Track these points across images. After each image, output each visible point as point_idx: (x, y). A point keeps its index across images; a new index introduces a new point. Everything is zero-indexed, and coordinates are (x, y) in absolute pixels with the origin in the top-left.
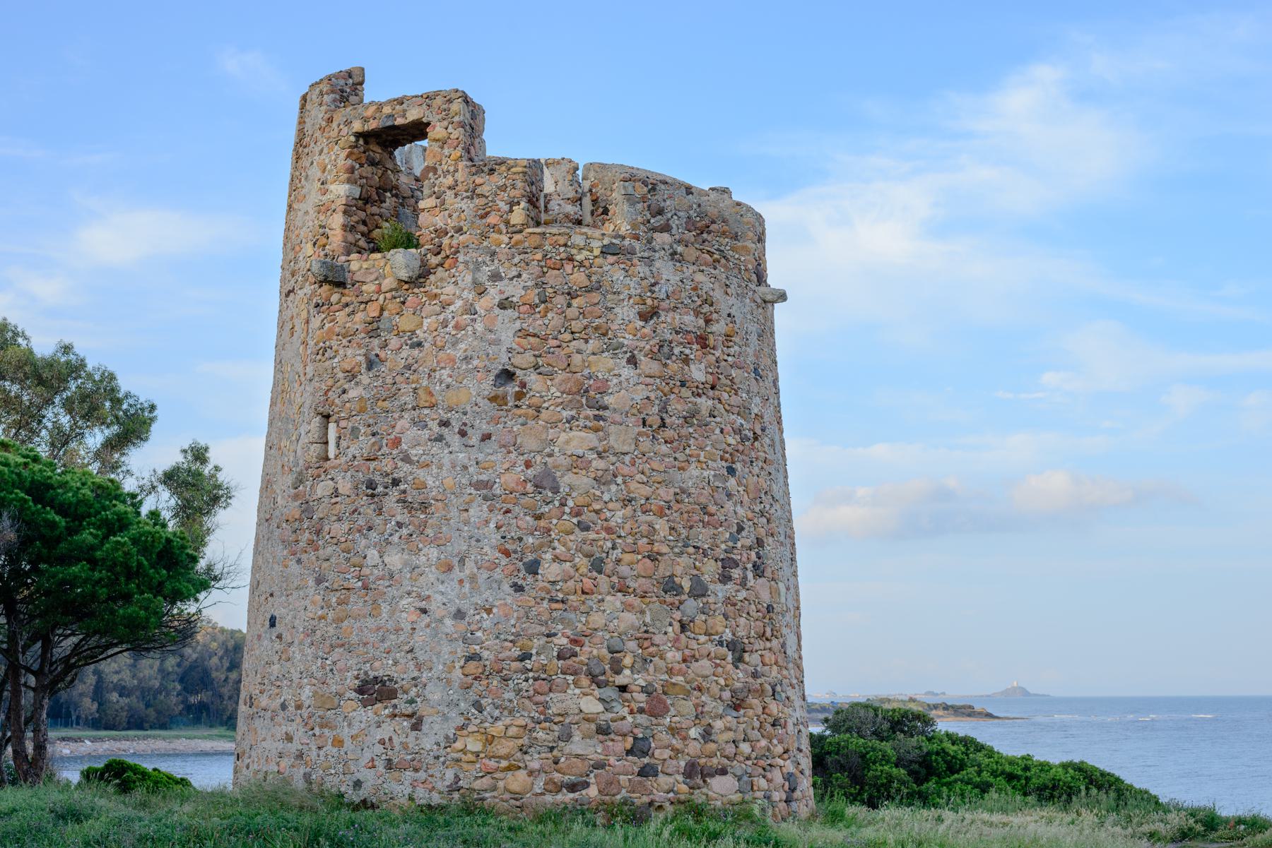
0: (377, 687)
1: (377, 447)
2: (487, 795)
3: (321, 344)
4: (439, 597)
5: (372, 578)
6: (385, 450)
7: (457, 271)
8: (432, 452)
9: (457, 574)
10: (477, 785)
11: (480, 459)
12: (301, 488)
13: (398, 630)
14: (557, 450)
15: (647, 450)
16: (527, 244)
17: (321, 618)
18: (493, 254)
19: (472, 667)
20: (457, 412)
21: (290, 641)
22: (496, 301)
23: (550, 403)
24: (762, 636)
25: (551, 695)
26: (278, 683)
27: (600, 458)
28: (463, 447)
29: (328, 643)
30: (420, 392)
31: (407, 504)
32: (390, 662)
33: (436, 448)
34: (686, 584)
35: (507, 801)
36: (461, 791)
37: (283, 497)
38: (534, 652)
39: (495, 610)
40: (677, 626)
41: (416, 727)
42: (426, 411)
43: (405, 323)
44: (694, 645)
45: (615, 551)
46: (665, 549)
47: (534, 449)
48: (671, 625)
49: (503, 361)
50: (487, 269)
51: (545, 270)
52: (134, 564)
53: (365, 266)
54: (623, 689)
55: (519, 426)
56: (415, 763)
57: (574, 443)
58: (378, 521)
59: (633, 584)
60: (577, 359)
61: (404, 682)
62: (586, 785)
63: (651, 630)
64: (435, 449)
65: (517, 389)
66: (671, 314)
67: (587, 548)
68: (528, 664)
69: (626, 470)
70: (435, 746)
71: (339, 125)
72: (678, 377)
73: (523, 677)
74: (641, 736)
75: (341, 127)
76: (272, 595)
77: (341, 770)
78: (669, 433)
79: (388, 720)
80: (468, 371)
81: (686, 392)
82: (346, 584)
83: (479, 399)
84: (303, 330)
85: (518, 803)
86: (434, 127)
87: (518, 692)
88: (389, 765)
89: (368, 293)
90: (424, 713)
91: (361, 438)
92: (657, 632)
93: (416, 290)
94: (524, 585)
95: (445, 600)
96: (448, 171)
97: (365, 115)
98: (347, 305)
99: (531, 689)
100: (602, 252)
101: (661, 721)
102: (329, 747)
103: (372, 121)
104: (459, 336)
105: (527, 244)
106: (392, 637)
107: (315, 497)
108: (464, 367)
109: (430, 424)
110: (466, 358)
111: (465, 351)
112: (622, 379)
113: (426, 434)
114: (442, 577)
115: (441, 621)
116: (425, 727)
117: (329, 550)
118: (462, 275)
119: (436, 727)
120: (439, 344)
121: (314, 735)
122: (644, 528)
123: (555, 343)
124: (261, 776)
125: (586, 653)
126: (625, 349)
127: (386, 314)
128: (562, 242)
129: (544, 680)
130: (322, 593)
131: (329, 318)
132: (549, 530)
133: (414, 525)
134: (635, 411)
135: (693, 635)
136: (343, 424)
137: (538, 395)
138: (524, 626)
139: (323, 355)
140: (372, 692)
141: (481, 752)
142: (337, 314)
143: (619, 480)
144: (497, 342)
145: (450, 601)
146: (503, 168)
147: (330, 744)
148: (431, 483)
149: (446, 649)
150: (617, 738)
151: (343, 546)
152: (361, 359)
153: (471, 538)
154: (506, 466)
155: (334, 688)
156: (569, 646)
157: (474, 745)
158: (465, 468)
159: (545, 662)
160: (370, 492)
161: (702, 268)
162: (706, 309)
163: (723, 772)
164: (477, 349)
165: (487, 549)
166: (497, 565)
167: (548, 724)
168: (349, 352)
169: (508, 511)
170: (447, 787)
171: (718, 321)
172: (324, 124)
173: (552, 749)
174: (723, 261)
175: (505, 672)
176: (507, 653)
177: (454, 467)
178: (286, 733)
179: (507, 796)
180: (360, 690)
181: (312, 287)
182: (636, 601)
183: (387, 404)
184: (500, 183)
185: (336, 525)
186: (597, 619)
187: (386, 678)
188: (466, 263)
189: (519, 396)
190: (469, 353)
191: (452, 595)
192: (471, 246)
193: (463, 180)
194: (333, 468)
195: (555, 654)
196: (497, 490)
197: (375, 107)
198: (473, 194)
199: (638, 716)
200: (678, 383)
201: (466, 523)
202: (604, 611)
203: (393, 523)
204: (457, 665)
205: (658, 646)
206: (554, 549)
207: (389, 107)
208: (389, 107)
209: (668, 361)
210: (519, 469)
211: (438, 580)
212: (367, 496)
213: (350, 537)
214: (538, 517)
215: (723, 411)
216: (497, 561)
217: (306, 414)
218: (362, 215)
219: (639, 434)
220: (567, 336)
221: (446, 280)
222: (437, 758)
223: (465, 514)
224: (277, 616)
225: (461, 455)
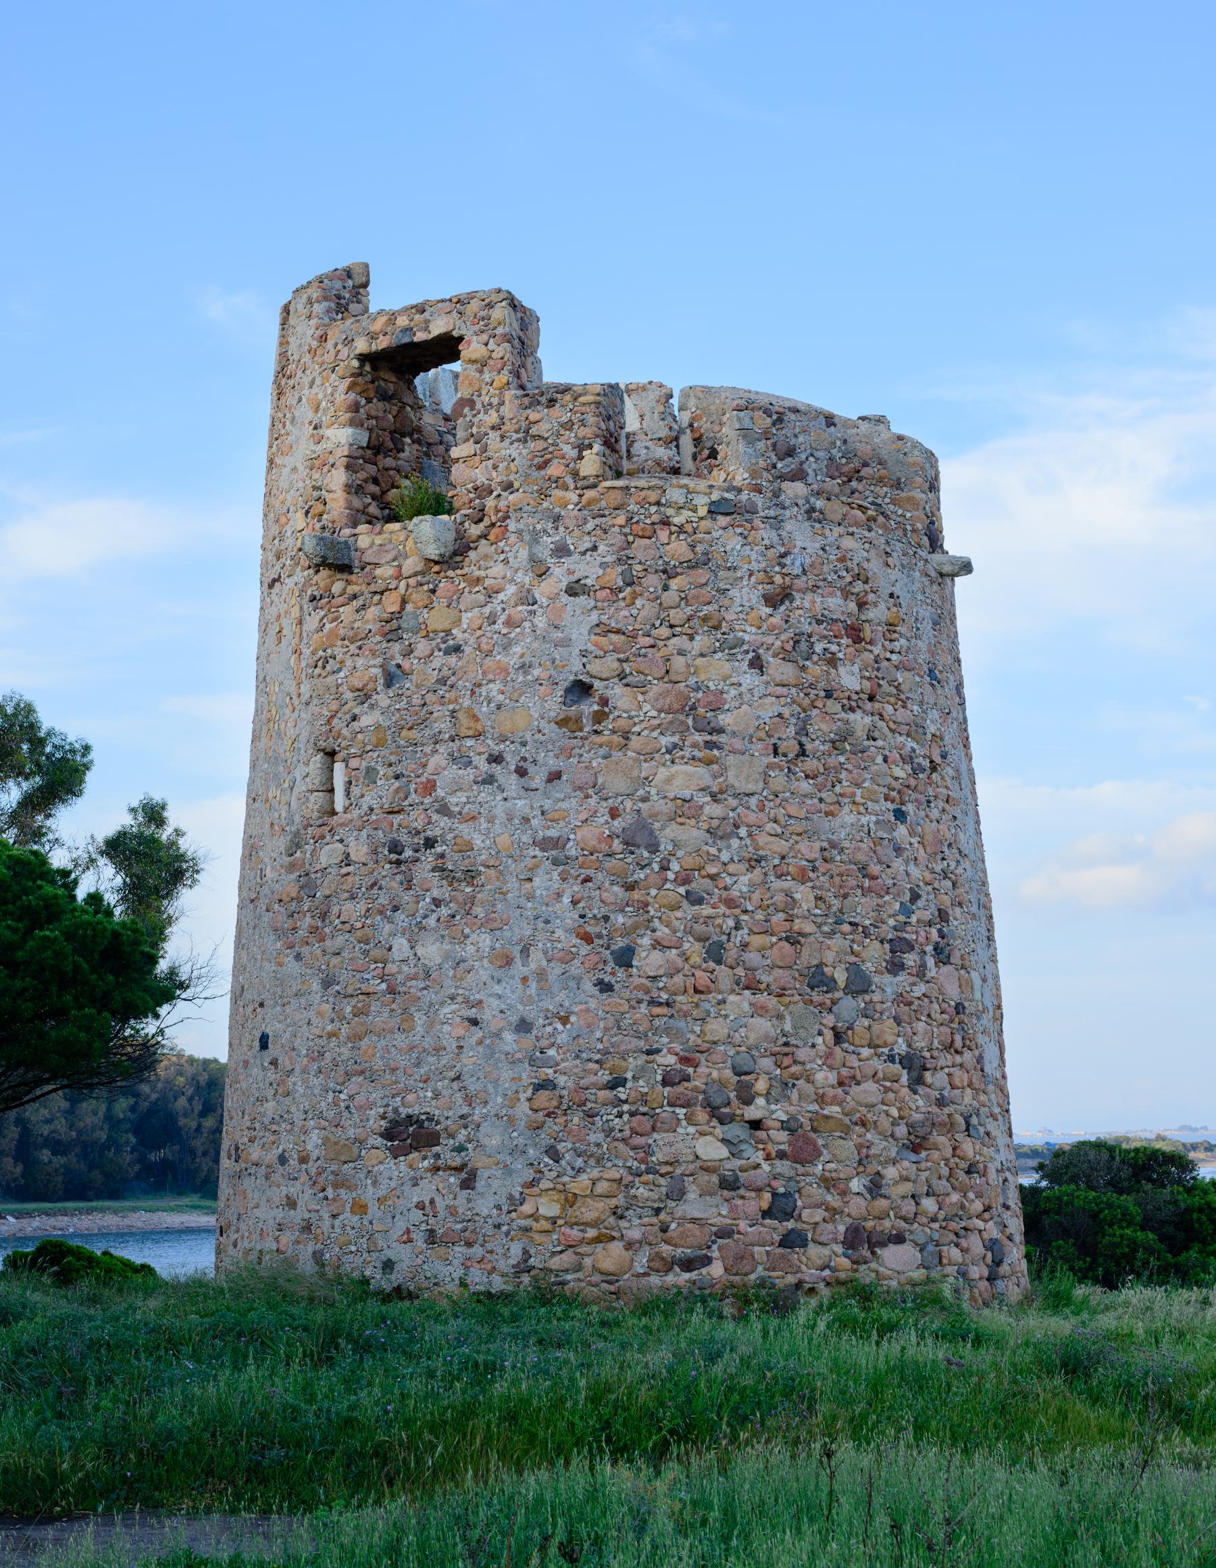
0: (411, 1129)
1: (402, 795)
2: (569, 1277)
3: (321, 653)
4: (495, 1003)
5: (400, 978)
6: (414, 798)
8: (480, 799)
9: (518, 969)
10: (555, 1263)
11: (546, 807)
12: (298, 854)
13: (438, 1050)
14: (653, 791)
15: (780, 788)
16: (603, 504)
17: (331, 1035)
18: (557, 519)
19: (543, 1097)
20: (513, 742)
22: (563, 585)
23: (643, 726)
24: (949, 1047)
25: (655, 1135)
26: (274, 1127)
28: (522, 793)
29: (341, 1069)
30: (460, 715)
31: (446, 873)
32: (429, 1094)
33: (484, 794)
34: (841, 976)
35: (596, 1285)
36: (533, 1273)
37: (273, 868)
38: (629, 1075)
39: (573, 1019)
40: (829, 1035)
41: (468, 1184)
42: (470, 742)
43: (437, 619)
44: (853, 1061)
45: (740, 932)
46: (809, 928)
48: (820, 1033)
49: (575, 669)
50: (549, 540)
51: (631, 538)
52: (70, 968)
53: (378, 541)
54: (756, 1125)
55: (600, 760)
56: (467, 1234)
57: (676, 782)
58: (407, 897)
59: (765, 978)
60: (679, 663)
61: (449, 1122)
62: (707, 1261)
63: (793, 1041)
64: (483, 794)
65: (596, 707)
66: (809, 596)
67: (699, 928)
68: (622, 1093)
69: (752, 818)
70: (495, 1211)
71: (336, 345)
72: (822, 685)
73: (615, 1111)
74: (782, 1190)
75: (339, 347)
76: (261, 1005)
77: (365, 1246)
78: (811, 764)
79: (429, 1175)
80: (526, 684)
81: (833, 706)
83: (543, 724)
84: (294, 633)
85: (612, 1288)
86: (469, 342)
87: (609, 1132)
88: (431, 1237)
89: (385, 580)
90: (479, 1165)
91: (379, 783)
92: (800, 1043)
93: (450, 573)
94: (613, 982)
95: (503, 1007)
96: (490, 404)
97: (372, 329)
98: (355, 597)
99: (627, 1127)
100: (709, 512)
101: (809, 1169)
102: (347, 1214)
103: (381, 337)
104: (512, 635)
105: (603, 504)
106: (430, 1059)
108: (521, 678)
109: (476, 760)
110: (523, 666)
111: (522, 656)
112: (742, 689)
113: (470, 774)
114: (498, 974)
115: (497, 1035)
116: (480, 1184)
117: (340, 940)
118: (514, 550)
119: (496, 1183)
120: (484, 647)
121: (326, 1198)
122: (779, 898)
123: (648, 641)
124: (253, 1257)
125: (706, 1073)
126: (745, 647)
127: (409, 607)
128: (653, 499)
129: (644, 1114)
130: (331, 999)
131: (330, 616)
132: (647, 905)
133: (458, 903)
134: (762, 734)
135: (851, 1048)
136: (354, 763)
137: (625, 715)
138: (614, 1039)
139: (324, 667)
140: (405, 1136)
141: (559, 1217)
142: (341, 609)
143: (743, 832)
144: (566, 643)
145: (510, 1007)
146: (568, 397)
147: (348, 1209)
148: (479, 842)
149: (506, 1074)
150: (748, 1194)
151: (359, 934)
154: (583, 816)
155: (351, 1133)
156: (678, 1066)
157: (549, 1208)
158: (526, 820)
159: (645, 1090)
160: (394, 857)
161: (851, 529)
162: (859, 587)
163: (899, 1239)
165: (559, 933)
166: (574, 956)
167: (651, 1176)
168: (360, 662)
169: (588, 880)
170: (513, 1266)
171: (875, 604)
172: (315, 344)
174: (881, 519)
175: (589, 1105)
176: (593, 1079)
177: (510, 819)
178: (288, 1197)
179: (597, 1278)
180: (388, 1135)
181: (306, 573)
182: (771, 1002)
183: (414, 734)
184: (564, 419)
185: (349, 905)
186: (718, 1029)
187: (424, 1117)
188: (519, 533)
189: (599, 717)
190: (527, 659)
191: (513, 998)
192: (526, 508)
193: (511, 416)
194: (342, 825)
195: (659, 1078)
196: (572, 850)
197: (385, 318)
198: (527, 435)
199: (777, 1162)
200: (822, 694)
201: (530, 897)
202: (726, 1016)
203: (428, 900)
204: (523, 1096)
205: (803, 1063)
206: (654, 931)
209: (807, 663)
210: (602, 820)
211: (493, 978)
212: (391, 863)
214: (630, 887)
215: (886, 731)
216: (573, 950)
217: (302, 751)
218: (372, 469)
219: (770, 766)
220: (664, 632)
221: (492, 558)
222: (498, 1226)
223: (528, 885)
224: (271, 1034)
225: (520, 803)
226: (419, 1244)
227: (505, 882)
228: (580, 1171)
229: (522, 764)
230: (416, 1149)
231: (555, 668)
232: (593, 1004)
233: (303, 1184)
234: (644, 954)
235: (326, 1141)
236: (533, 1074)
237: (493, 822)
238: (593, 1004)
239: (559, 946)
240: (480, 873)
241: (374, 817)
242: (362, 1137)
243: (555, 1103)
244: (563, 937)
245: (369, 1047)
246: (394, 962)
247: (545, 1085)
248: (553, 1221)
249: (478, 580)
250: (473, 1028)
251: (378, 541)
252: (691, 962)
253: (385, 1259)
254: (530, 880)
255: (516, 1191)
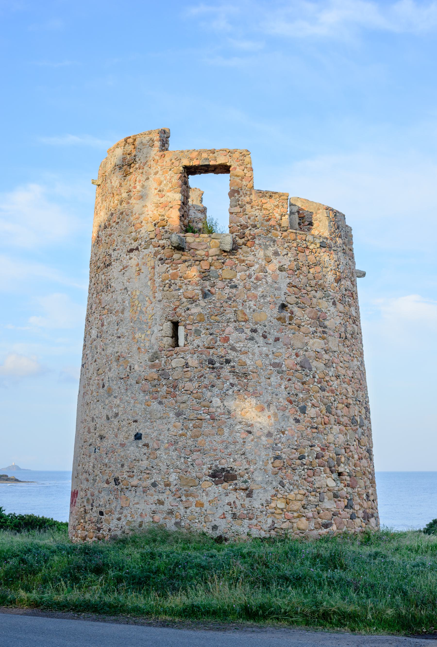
0: (224, 474)
1: (214, 341)
3: (167, 281)
4: (258, 425)
6: (219, 343)
7: (255, 248)
8: (248, 346)
10: (284, 526)
11: (274, 351)
12: (157, 361)
13: (235, 443)
14: (309, 348)
16: (289, 238)
17: (181, 435)
19: (278, 463)
20: (260, 325)
21: (157, 448)
22: (277, 267)
26: (148, 472)
27: (326, 353)
28: (265, 345)
29: (188, 449)
30: (239, 312)
31: (236, 374)
32: (232, 460)
33: (250, 344)
35: (298, 534)
36: (276, 530)
37: (139, 366)
38: (306, 454)
39: (286, 432)
41: (249, 495)
42: (243, 323)
43: (226, 273)
45: (335, 402)
47: (300, 347)
48: (355, 441)
55: (291, 335)
56: (250, 515)
57: (316, 345)
59: (342, 419)
61: (240, 471)
62: (331, 524)
63: (350, 444)
64: (249, 344)
65: (289, 315)
67: (325, 400)
68: (304, 461)
70: (260, 506)
73: (302, 468)
74: (350, 498)
75: (173, 161)
76: (136, 421)
77: (203, 520)
79: (233, 492)
80: (265, 303)
82: (199, 417)
83: (272, 319)
85: (303, 535)
86: (235, 168)
87: (300, 476)
88: (234, 516)
89: (201, 256)
90: (254, 488)
91: (202, 336)
93: (231, 257)
94: (300, 419)
95: (261, 427)
96: (246, 194)
98: (185, 261)
99: (306, 474)
100: (320, 246)
102: (193, 507)
103: (195, 160)
104: (258, 284)
105: (289, 238)
107: (170, 367)
108: (262, 301)
109: (246, 330)
110: (263, 296)
111: (262, 292)
112: (331, 312)
113: (243, 336)
114: (259, 414)
115: (259, 438)
116: (254, 496)
118: (258, 251)
119: (261, 495)
120: (247, 287)
121: (182, 501)
123: (304, 291)
124: (137, 524)
125: (328, 454)
128: (304, 238)
129: (310, 469)
130: (181, 421)
132: (309, 390)
133: (241, 385)
136: (189, 327)
137: (299, 318)
138: (301, 441)
139: (170, 288)
140: (221, 476)
141: (284, 508)
142: (179, 265)
143: (334, 365)
144: (279, 289)
146: (277, 196)
147: (194, 505)
148: (249, 362)
149: (263, 453)
151: (195, 395)
152: (200, 292)
153: (273, 393)
154: (287, 355)
155: (194, 475)
156: (321, 452)
157: (281, 505)
158: (267, 355)
160: (211, 366)
164: (269, 292)
165: (281, 399)
167: (314, 493)
169: (290, 380)
170: (269, 527)
172: (157, 158)
173: (316, 505)
176: (294, 456)
177: (261, 355)
181: (156, 249)
182: (344, 428)
183: (218, 318)
184: (276, 204)
185: (189, 384)
186: (331, 438)
187: (229, 469)
188: (260, 245)
190: (265, 294)
192: (262, 236)
193: (255, 199)
194: (183, 351)
195: (315, 456)
197: (197, 153)
201: (270, 385)
203: (228, 384)
207: (206, 154)
208: (206, 154)
211: (257, 415)
212: (209, 368)
213: (200, 391)
214: (303, 383)
216: (286, 406)
221: (249, 253)
223: (269, 380)
224: (143, 434)
225: (265, 349)
226: (229, 519)
227: (260, 379)
228: (292, 490)
229: (264, 333)
230: (226, 481)
231: (276, 298)
232: (293, 427)
233: (168, 495)
234: (309, 409)
235: (180, 478)
236: (274, 453)
237: (254, 355)
238: (293, 427)
239: (281, 404)
240: (249, 374)
241: (200, 349)
242: (200, 476)
243: (282, 465)
244: (282, 401)
245: (202, 440)
246: (213, 407)
247: (277, 458)
248: (282, 510)
249: (243, 261)
250: (249, 435)
251: (197, 240)
252: (323, 413)
253: (213, 525)
254: (269, 378)
255: (269, 498)
